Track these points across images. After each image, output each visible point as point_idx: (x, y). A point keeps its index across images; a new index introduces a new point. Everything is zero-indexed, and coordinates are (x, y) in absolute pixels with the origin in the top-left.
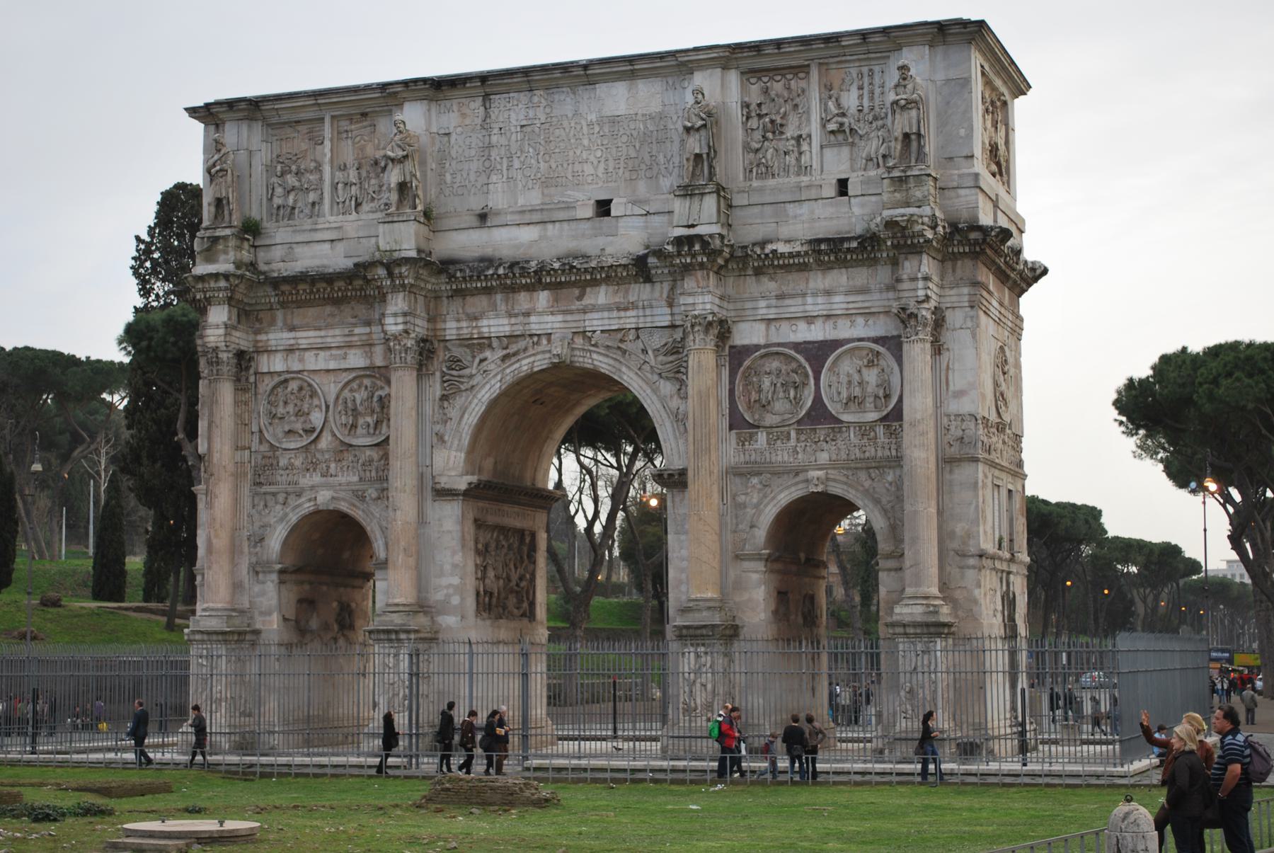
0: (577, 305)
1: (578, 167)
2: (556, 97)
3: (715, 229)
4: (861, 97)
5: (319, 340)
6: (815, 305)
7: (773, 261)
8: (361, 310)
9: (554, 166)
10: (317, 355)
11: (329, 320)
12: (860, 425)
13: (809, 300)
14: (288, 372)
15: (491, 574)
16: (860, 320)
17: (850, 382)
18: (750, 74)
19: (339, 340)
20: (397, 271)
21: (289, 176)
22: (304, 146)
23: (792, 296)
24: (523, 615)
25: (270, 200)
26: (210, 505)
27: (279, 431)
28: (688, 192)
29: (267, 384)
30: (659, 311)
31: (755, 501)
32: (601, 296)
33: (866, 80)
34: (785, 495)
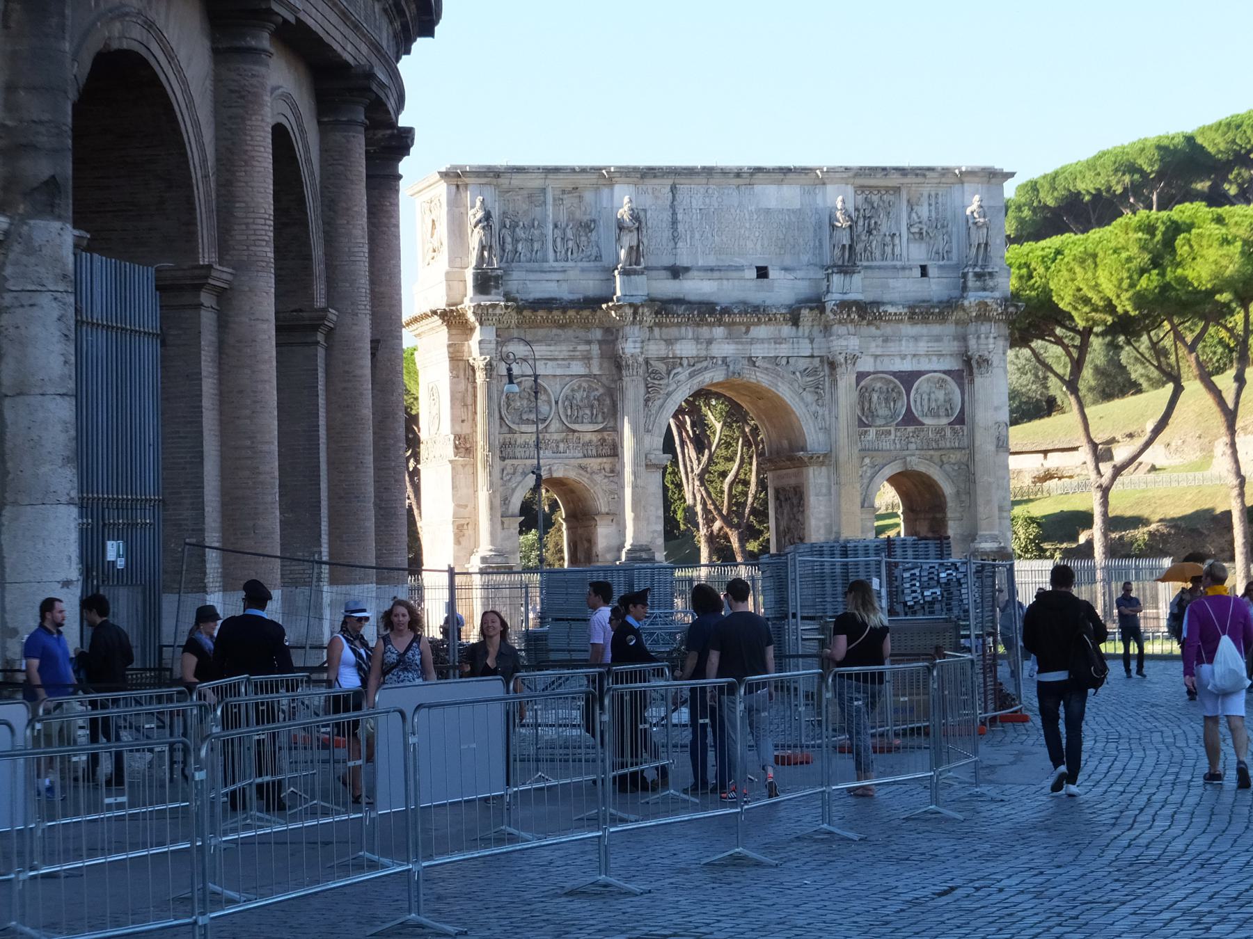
2: (726, 191)
4: (930, 211)
5: (549, 353)
6: (907, 347)
7: (881, 319)
8: (582, 334)
9: (725, 240)
10: (546, 364)
13: (904, 343)
14: (523, 376)
16: (935, 359)
17: (929, 399)
18: (862, 188)
19: (565, 354)
20: (640, 310)
21: (517, 229)
22: (525, 207)
23: (894, 341)
31: (868, 475)
32: (761, 331)
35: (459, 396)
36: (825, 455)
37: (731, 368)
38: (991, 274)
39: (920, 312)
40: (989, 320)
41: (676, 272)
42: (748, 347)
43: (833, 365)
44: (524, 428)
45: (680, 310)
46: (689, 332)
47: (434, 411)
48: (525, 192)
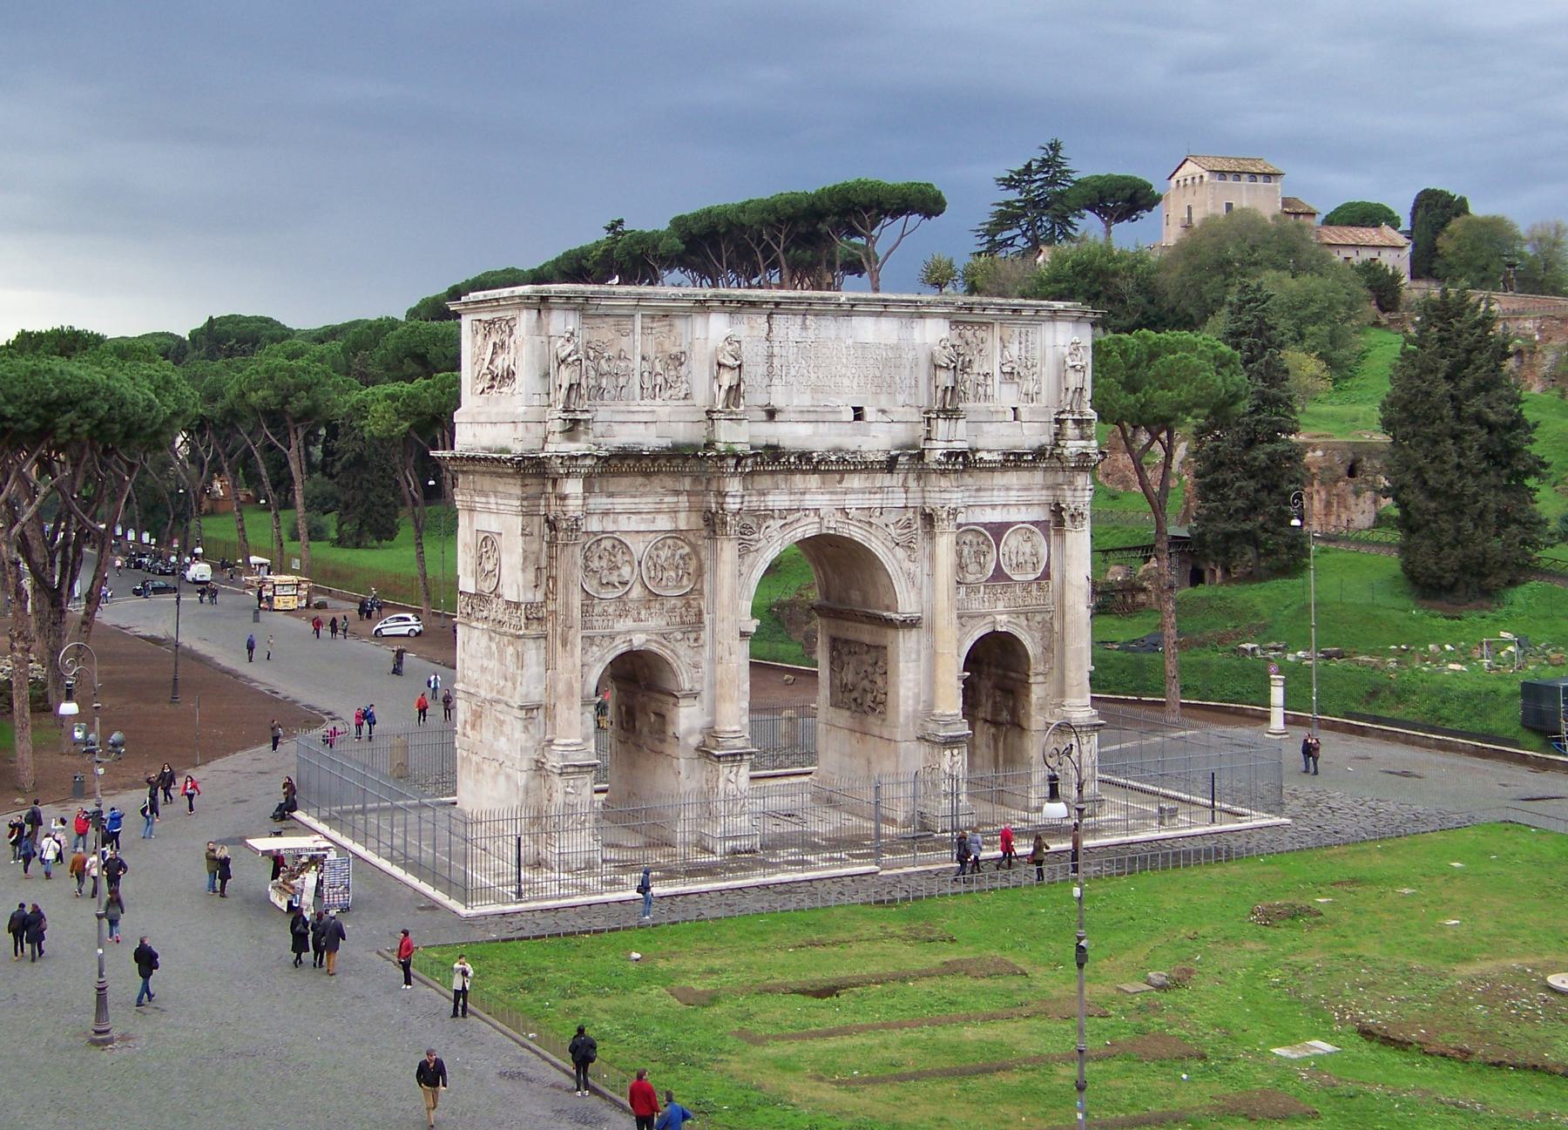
0: (839, 488)
1: (838, 379)
2: (823, 322)
6: (998, 497)
8: (669, 482)
11: (641, 489)
12: (1023, 582)
13: (995, 493)
14: (603, 532)
16: (1023, 508)
18: (955, 323)
21: (603, 361)
23: (985, 490)
27: (595, 582)
30: (896, 496)
32: (855, 481)
35: (532, 557)
36: (919, 618)
37: (825, 523)
39: (1014, 460)
42: (843, 497)
43: (929, 519)
47: (488, 567)
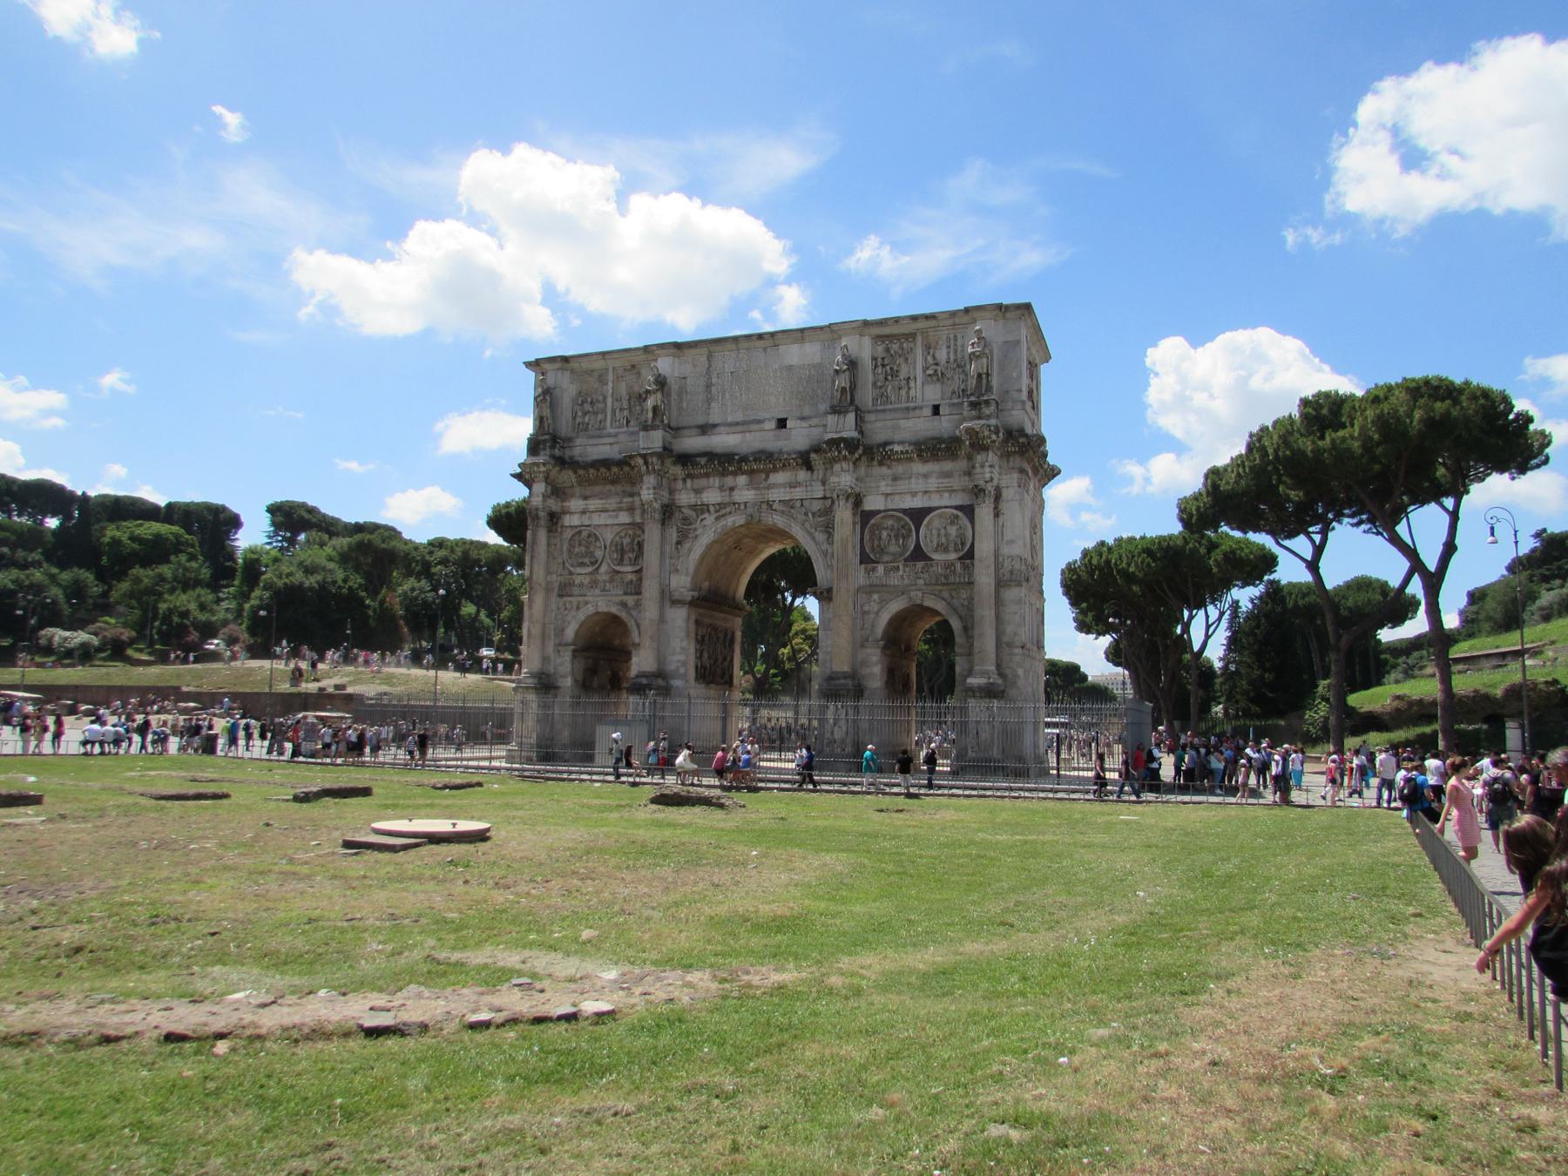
3: (855, 434)
4: (948, 353)
6: (917, 484)
8: (628, 488)
13: (913, 480)
15: (706, 655)
16: (946, 495)
18: (879, 338)
19: (614, 506)
23: (901, 479)
24: (726, 683)
25: (574, 418)
26: (530, 607)
28: (836, 410)
29: (568, 534)
32: (780, 477)
33: (952, 342)
34: (896, 606)
38: (987, 402)
40: (985, 448)
41: (705, 429)
44: (579, 570)
45: (703, 461)
46: (715, 481)
48: (596, 374)
